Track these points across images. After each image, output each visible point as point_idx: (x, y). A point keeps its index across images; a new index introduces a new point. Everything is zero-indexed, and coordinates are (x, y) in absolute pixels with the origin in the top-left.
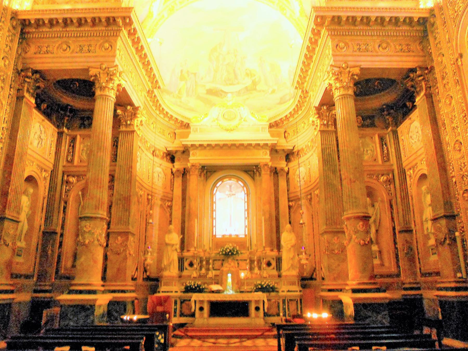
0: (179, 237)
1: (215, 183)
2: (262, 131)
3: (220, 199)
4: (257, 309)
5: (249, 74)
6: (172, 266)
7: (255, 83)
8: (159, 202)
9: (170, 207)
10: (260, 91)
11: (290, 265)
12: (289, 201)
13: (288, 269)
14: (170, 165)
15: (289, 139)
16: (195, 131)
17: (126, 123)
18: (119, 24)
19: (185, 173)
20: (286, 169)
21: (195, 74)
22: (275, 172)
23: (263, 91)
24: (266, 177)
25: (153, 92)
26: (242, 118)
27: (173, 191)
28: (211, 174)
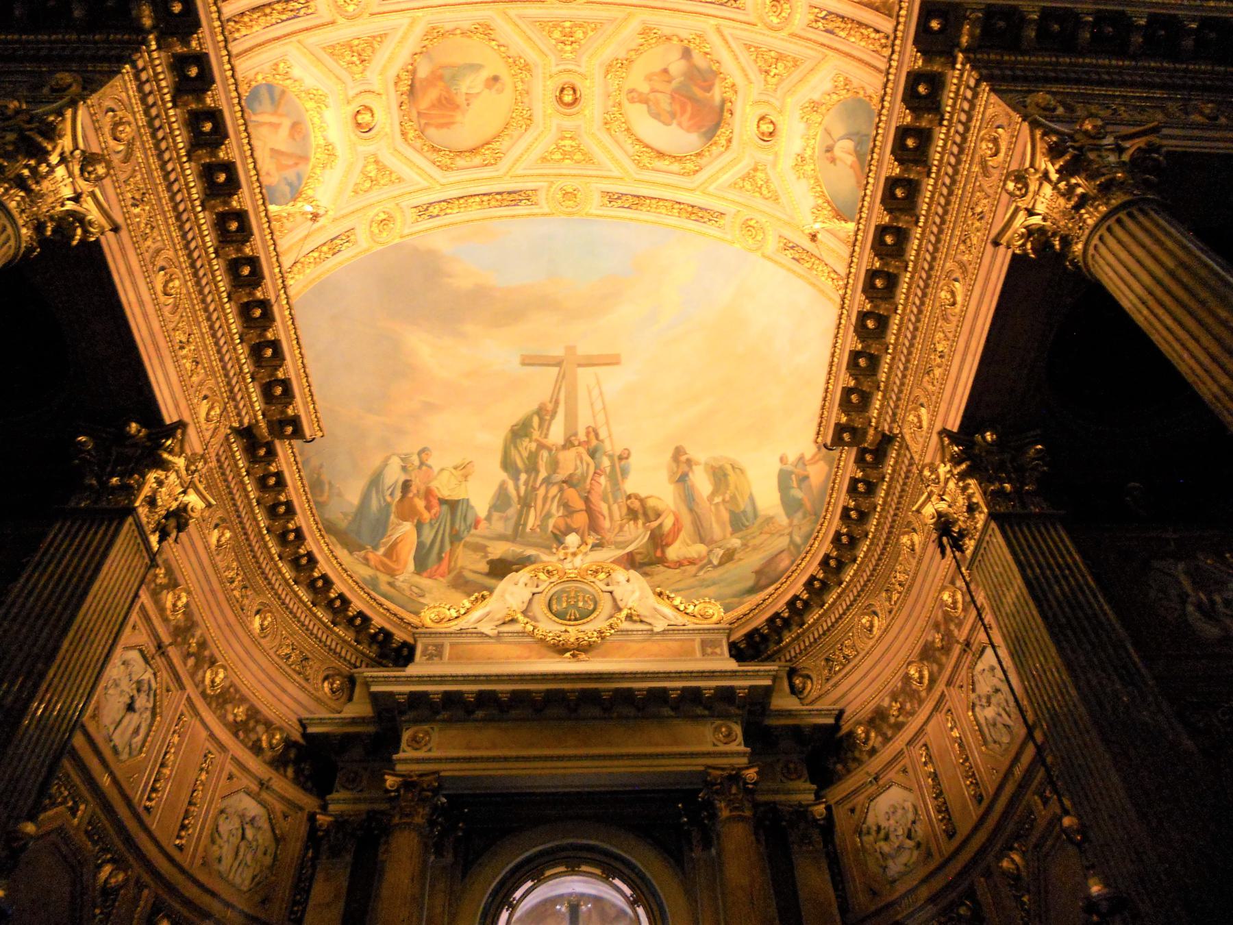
1: (502, 884)
2: (704, 653)
5: (639, 511)
7: (659, 540)
10: (679, 564)
14: (309, 802)
17: (104, 484)
20: (820, 809)
21: (453, 505)
23: (692, 562)
24: (737, 839)
26: (620, 610)
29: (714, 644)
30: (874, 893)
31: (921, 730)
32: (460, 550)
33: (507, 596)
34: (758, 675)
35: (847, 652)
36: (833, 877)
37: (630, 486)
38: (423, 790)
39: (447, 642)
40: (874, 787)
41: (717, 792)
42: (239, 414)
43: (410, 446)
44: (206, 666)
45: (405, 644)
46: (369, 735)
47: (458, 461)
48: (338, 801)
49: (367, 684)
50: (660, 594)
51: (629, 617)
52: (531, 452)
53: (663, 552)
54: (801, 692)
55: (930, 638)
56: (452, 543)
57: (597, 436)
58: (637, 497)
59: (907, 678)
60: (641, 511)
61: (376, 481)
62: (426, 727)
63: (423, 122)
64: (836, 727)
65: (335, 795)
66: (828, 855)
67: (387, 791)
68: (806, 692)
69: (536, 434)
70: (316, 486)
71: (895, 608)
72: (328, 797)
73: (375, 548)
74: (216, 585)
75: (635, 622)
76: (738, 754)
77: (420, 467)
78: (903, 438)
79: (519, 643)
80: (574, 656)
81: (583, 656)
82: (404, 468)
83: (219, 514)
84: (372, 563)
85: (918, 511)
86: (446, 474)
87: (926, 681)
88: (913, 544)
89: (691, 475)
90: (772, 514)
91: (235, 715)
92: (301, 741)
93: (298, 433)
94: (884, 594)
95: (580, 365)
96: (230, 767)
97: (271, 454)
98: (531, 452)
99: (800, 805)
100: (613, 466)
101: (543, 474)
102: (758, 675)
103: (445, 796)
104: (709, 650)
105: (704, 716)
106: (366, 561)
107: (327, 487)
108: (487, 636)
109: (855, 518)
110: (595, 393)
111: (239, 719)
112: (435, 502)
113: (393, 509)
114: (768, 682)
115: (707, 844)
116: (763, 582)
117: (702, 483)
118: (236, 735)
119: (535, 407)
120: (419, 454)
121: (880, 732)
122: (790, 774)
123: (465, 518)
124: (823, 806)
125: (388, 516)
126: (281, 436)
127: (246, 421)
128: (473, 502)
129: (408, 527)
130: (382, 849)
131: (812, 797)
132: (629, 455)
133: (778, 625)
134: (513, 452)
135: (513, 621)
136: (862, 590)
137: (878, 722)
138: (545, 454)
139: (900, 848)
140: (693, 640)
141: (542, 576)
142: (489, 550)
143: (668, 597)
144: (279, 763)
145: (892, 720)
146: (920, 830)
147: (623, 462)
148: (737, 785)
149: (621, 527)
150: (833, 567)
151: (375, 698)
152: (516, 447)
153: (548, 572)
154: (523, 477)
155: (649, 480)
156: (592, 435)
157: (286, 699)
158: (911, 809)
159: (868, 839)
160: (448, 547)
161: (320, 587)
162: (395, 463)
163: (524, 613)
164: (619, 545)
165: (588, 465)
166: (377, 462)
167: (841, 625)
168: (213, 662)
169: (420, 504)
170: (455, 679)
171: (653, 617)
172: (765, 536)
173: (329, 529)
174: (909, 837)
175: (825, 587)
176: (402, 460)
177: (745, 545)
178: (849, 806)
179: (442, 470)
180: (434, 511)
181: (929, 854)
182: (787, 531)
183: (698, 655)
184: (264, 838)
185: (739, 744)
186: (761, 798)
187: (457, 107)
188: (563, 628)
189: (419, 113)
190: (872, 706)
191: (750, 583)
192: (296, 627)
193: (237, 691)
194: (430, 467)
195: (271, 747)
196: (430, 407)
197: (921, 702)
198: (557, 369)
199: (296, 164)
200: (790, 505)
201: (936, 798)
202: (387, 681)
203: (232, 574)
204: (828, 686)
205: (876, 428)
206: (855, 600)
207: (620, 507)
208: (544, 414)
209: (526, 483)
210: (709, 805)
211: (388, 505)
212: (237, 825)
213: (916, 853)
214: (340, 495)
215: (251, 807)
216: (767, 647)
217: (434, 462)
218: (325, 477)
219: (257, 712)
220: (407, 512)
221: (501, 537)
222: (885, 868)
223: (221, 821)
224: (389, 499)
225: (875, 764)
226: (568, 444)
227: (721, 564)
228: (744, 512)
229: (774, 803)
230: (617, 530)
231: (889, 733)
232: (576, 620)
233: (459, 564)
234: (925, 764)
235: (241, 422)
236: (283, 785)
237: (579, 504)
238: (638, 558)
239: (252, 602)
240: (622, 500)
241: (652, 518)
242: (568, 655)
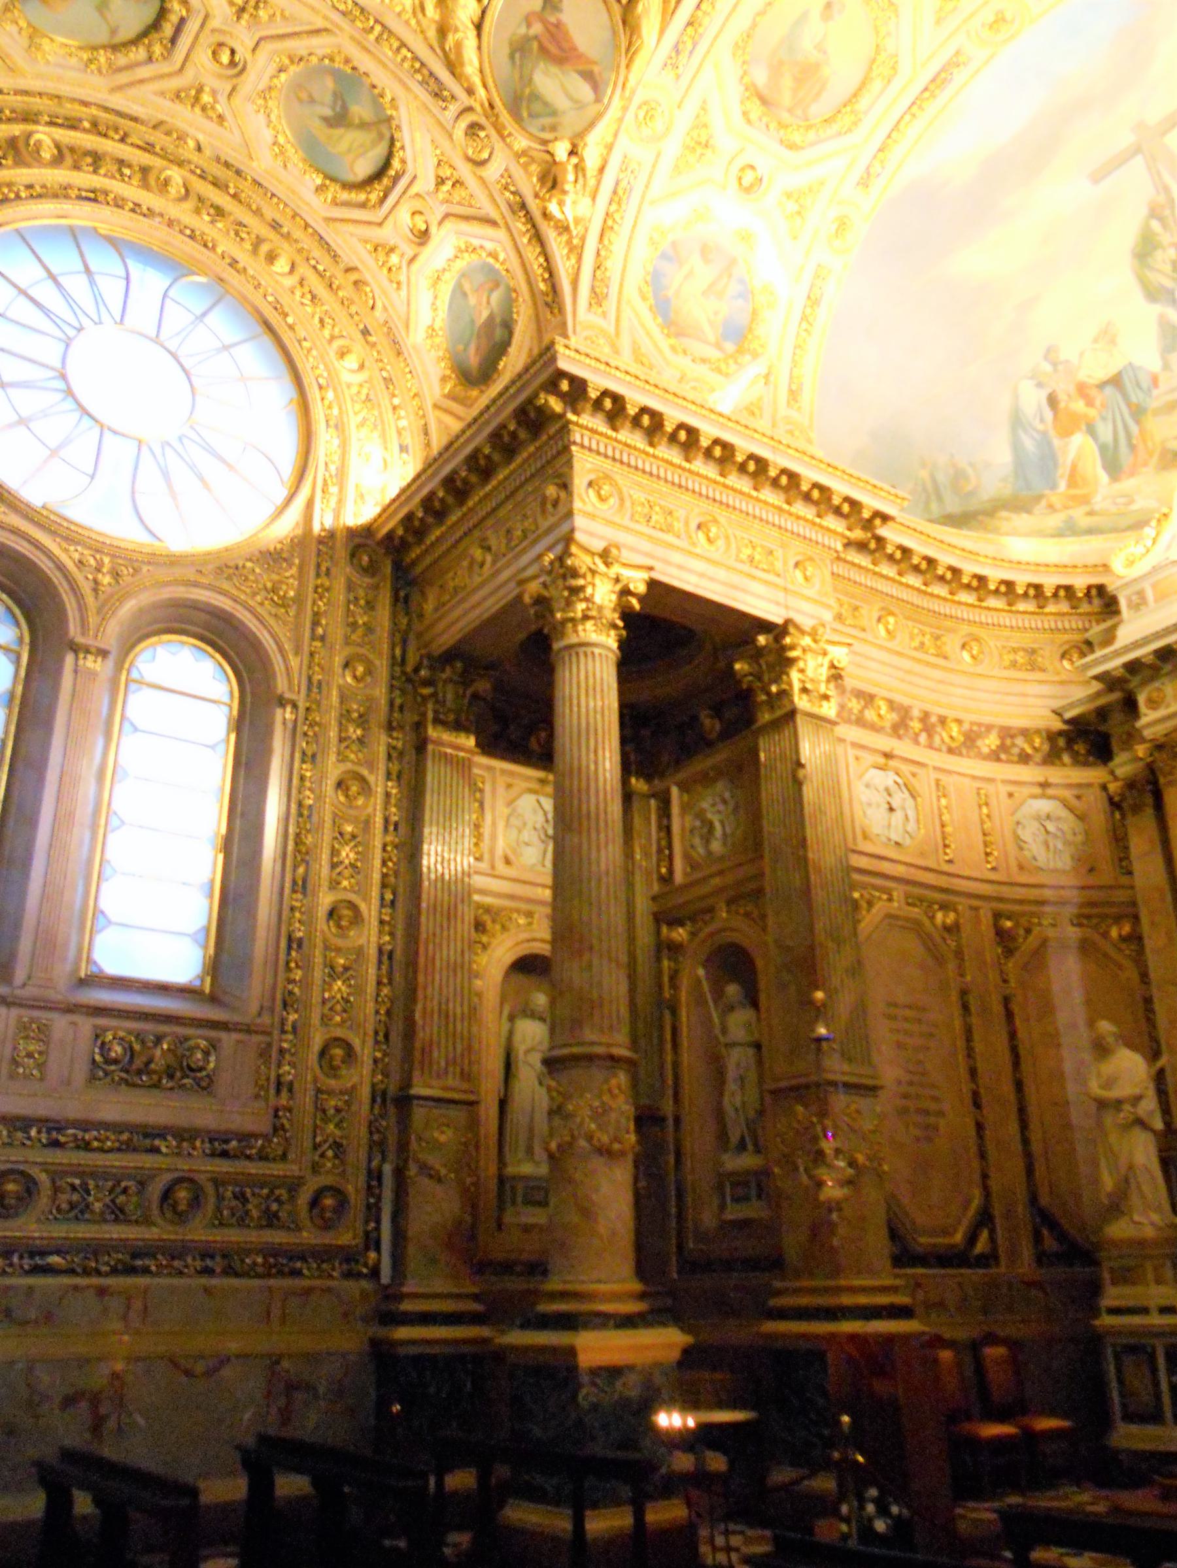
6: (1135, 1199)
8: (1073, 933)
14: (1094, 775)
17: (769, 694)
18: (553, 411)
21: (1116, 381)
25: (880, 540)
27: (1130, 873)
32: (1151, 423)
46: (1117, 701)
48: (1121, 765)
56: (1138, 422)
61: (1017, 421)
62: (1156, 684)
63: (799, 112)
73: (1054, 487)
82: (1040, 385)
84: (1058, 505)
92: (1065, 727)
95: (1164, 134)
106: (1051, 507)
107: (970, 471)
112: (1093, 392)
119: (1144, 211)
120: (1046, 358)
123: (1138, 385)
125: (1050, 444)
128: (1137, 362)
129: (1079, 440)
134: (1152, 276)
144: (1052, 758)
157: (1031, 701)
160: (1134, 429)
176: (1032, 378)
179: (1081, 354)
180: (1098, 403)
184: (1069, 823)
187: (817, 66)
189: (790, 111)
193: (980, 725)
194: (1067, 361)
198: (1139, 160)
199: (730, 276)
211: (1044, 434)
212: (1036, 824)
215: (1044, 806)
217: (1067, 353)
219: (1008, 728)
223: (1020, 832)
224: (1041, 427)
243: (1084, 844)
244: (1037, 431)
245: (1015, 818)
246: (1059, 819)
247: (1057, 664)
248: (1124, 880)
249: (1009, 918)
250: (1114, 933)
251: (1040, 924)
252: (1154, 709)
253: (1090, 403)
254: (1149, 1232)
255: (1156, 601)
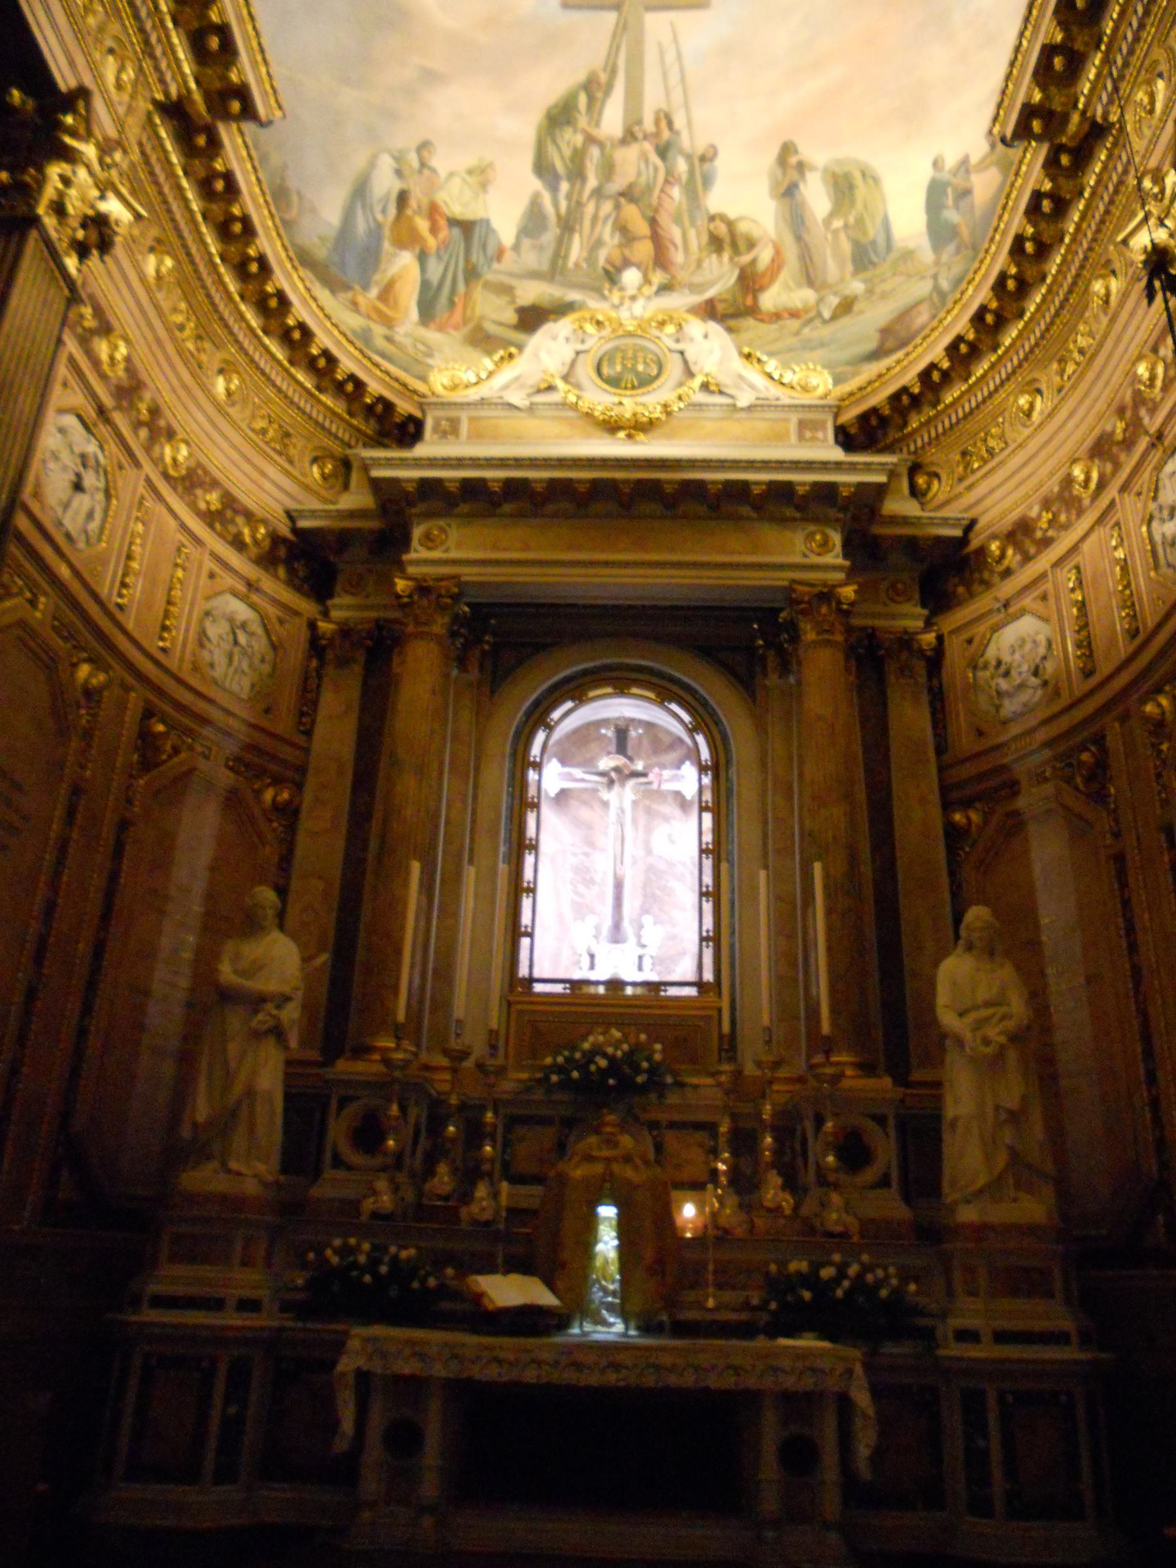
0: (306, 960)
1: (537, 703)
2: (801, 437)
3: (563, 795)
4: (799, 1456)
5: (725, 239)
6: (239, 1140)
7: (750, 282)
8: (225, 778)
9: (289, 814)
10: (776, 316)
11: (1002, 1159)
12: (947, 806)
13: (993, 1190)
14: (307, 607)
15: (939, 490)
16: (444, 434)
19: (375, 651)
20: (930, 638)
21: (466, 227)
22: (873, 660)
23: (794, 314)
27: (308, 733)
28: (520, 662)
29: (818, 426)
30: (980, 733)
31: (1074, 549)
32: (478, 293)
33: (543, 355)
34: (870, 468)
35: (992, 443)
36: (933, 714)
37: (717, 200)
38: (440, 596)
39: (464, 416)
40: (1002, 616)
41: (802, 612)
42: (162, 81)
43: (405, 139)
44: (163, 440)
45: (411, 418)
46: (371, 531)
47: (470, 161)
48: (341, 607)
49: (365, 468)
50: (748, 356)
51: (705, 387)
52: (575, 150)
53: (755, 299)
54: (924, 494)
55: (1109, 428)
56: (467, 282)
57: (670, 124)
58: (723, 218)
59: (1069, 480)
60: (727, 239)
61: (360, 190)
62: (441, 523)
64: (964, 541)
65: (337, 601)
66: (930, 689)
67: (398, 597)
68: (930, 495)
69: (582, 121)
70: (280, 195)
71: (1068, 385)
72: (329, 603)
73: (366, 287)
74: (162, 333)
75: (712, 392)
76: (834, 568)
77: (420, 172)
78: (1122, 129)
79: (560, 418)
80: (629, 436)
81: (641, 437)
82: (399, 173)
83: (154, 232)
85: (1125, 242)
86: (456, 182)
87: (1093, 485)
88: (1108, 294)
89: (801, 186)
90: (911, 245)
91: (208, 503)
92: (290, 536)
93: (248, 112)
94: (1055, 366)
96: (209, 565)
97: (214, 144)
98: (575, 150)
99: (906, 632)
100: (691, 172)
101: (592, 182)
102: (870, 468)
103: (469, 605)
104: (808, 434)
105: (795, 519)
106: (355, 306)
107: (295, 199)
108: (516, 408)
109: (1030, 253)
110: (670, 56)
111: (213, 508)
112: (442, 223)
113: (387, 232)
114: (882, 478)
115: (785, 668)
116: (890, 344)
117: (817, 198)
118: (211, 526)
119: (581, 76)
121: (1019, 547)
122: (896, 594)
123: (484, 247)
124: (933, 635)
126: (227, 116)
127: (173, 90)
128: (496, 224)
130: (396, 660)
131: (920, 624)
132: (715, 154)
133: (905, 403)
134: (551, 150)
135: (551, 388)
136: (1026, 358)
137: (1019, 536)
138: (595, 152)
139: (1022, 686)
140: (787, 420)
141: (590, 328)
142: (518, 292)
143: (759, 360)
145: (1039, 534)
146: (1050, 667)
147: (706, 166)
148: (829, 605)
149: (699, 264)
150: (989, 325)
151: (377, 485)
152: (554, 142)
153: (599, 323)
154: (564, 186)
155: (743, 195)
156: (663, 124)
157: (267, 486)
158: (1044, 643)
159: (983, 675)
160: (461, 287)
161: (297, 340)
162: (386, 164)
163: (566, 378)
164: (695, 288)
165: (656, 169)
166: (359, 162)
167: (989, 406)
168: (170, 434)
169: (423, 225)
170: (475, 462)
171: (738, 387)
172: (898, 280)
173: (304, 259)
174: (1036, 673)
175: (975, 352)
177: (870, 292)
178: (965, 636)
179: (451, 175)
181: (1057, 693)
182: (932, 271)
183: (793, 438)
184: (260, 645)
185: (837, 556)
186: (856, 622)
188: (616, 399)
190: (1014, 516)
191: (871, 345)
192: (270, 392)
193: (206, 472)
194: (434, 171)
195: (256, 542)
196: (431, 77)
197: (1080, 512)
200: (939, 232)
201: (1078, 632)
202: (390, 463)
203: (179, 319)
204: (961, 488)
205: (1084, 113)
206: (1014, 372)
207: (698, 234)
208: (594, 90)
209: (569, 197)
210: (792, 628)
211: (379, 226)
213: (1040, 692)
214: (314, 211)
215: (242, 611)
216: (885, 434)
217: (440, 163)
218: (292, 183)
220: (406, 238)
221: (534, 275)
222: (998, 708)
223: (208, 624)
224: (380, 217)
225: (1007, 588)
226: (629, 137)
227: (835, 317)
228: (874, 243)
229: (873, 628)
230: (693, 267)
231: (1032, 550)
232: (633, 388)
233: (478, 311)
234: (1073, 590)
235: (167, 93)
236: (274, 586)
237: (643, 228)
238: (720, 307)
239: (212, 358)
240: (702, 222)
241: (742, 245)
242: (622, 434)
243: (271, 676)
244: (375, 219)
245: (208, 606)
246: (252, 634)
247: (307, 465)
248: (300, 740)
249: (163, 722)
250: (268, 795)
251: (191, 748)
252: (429, 549)
253: (434, 230)
254: (251, 1187)
255: (469, 437)
